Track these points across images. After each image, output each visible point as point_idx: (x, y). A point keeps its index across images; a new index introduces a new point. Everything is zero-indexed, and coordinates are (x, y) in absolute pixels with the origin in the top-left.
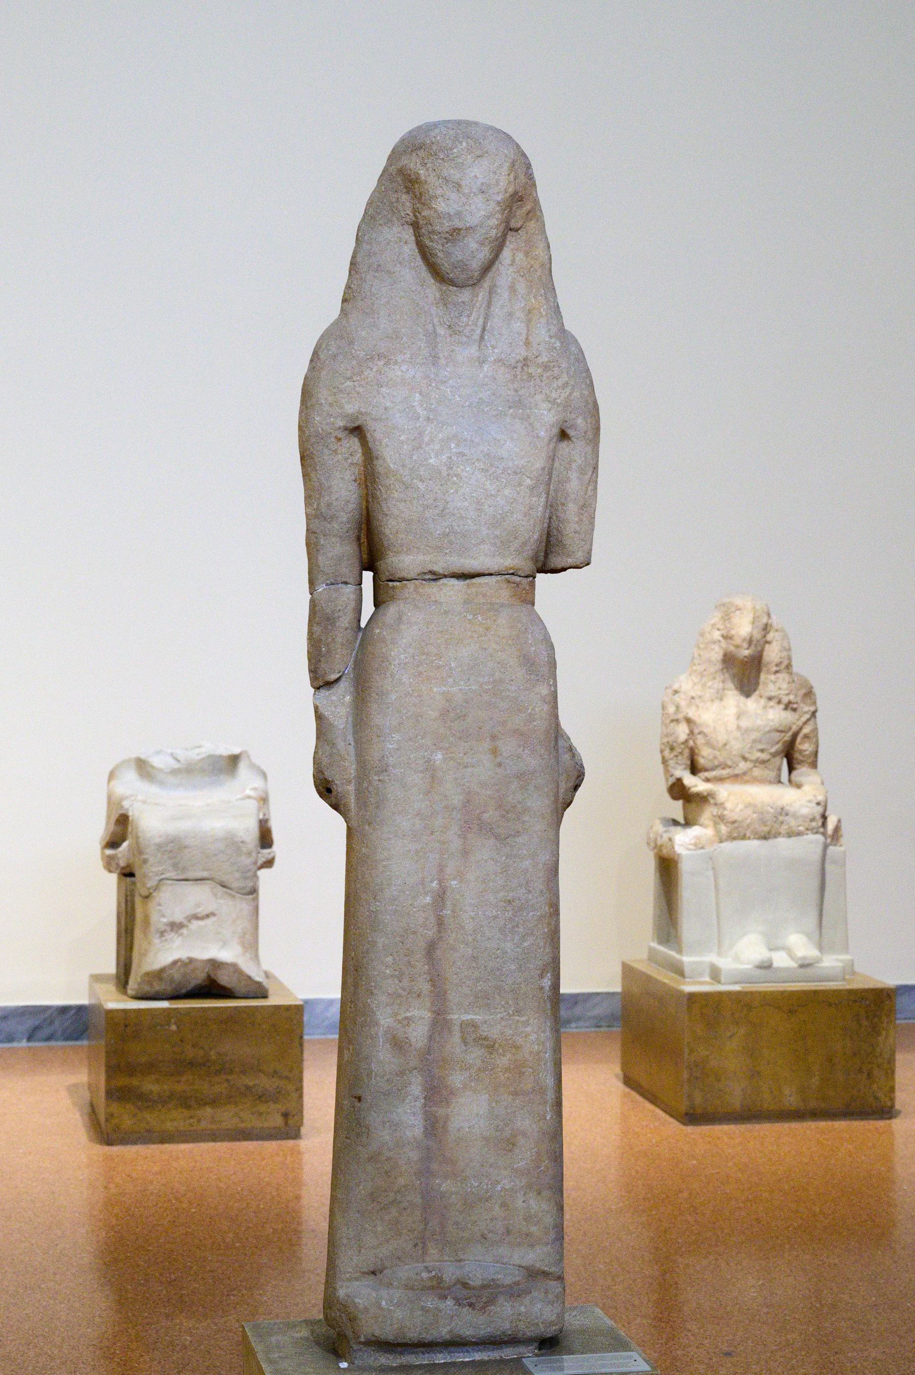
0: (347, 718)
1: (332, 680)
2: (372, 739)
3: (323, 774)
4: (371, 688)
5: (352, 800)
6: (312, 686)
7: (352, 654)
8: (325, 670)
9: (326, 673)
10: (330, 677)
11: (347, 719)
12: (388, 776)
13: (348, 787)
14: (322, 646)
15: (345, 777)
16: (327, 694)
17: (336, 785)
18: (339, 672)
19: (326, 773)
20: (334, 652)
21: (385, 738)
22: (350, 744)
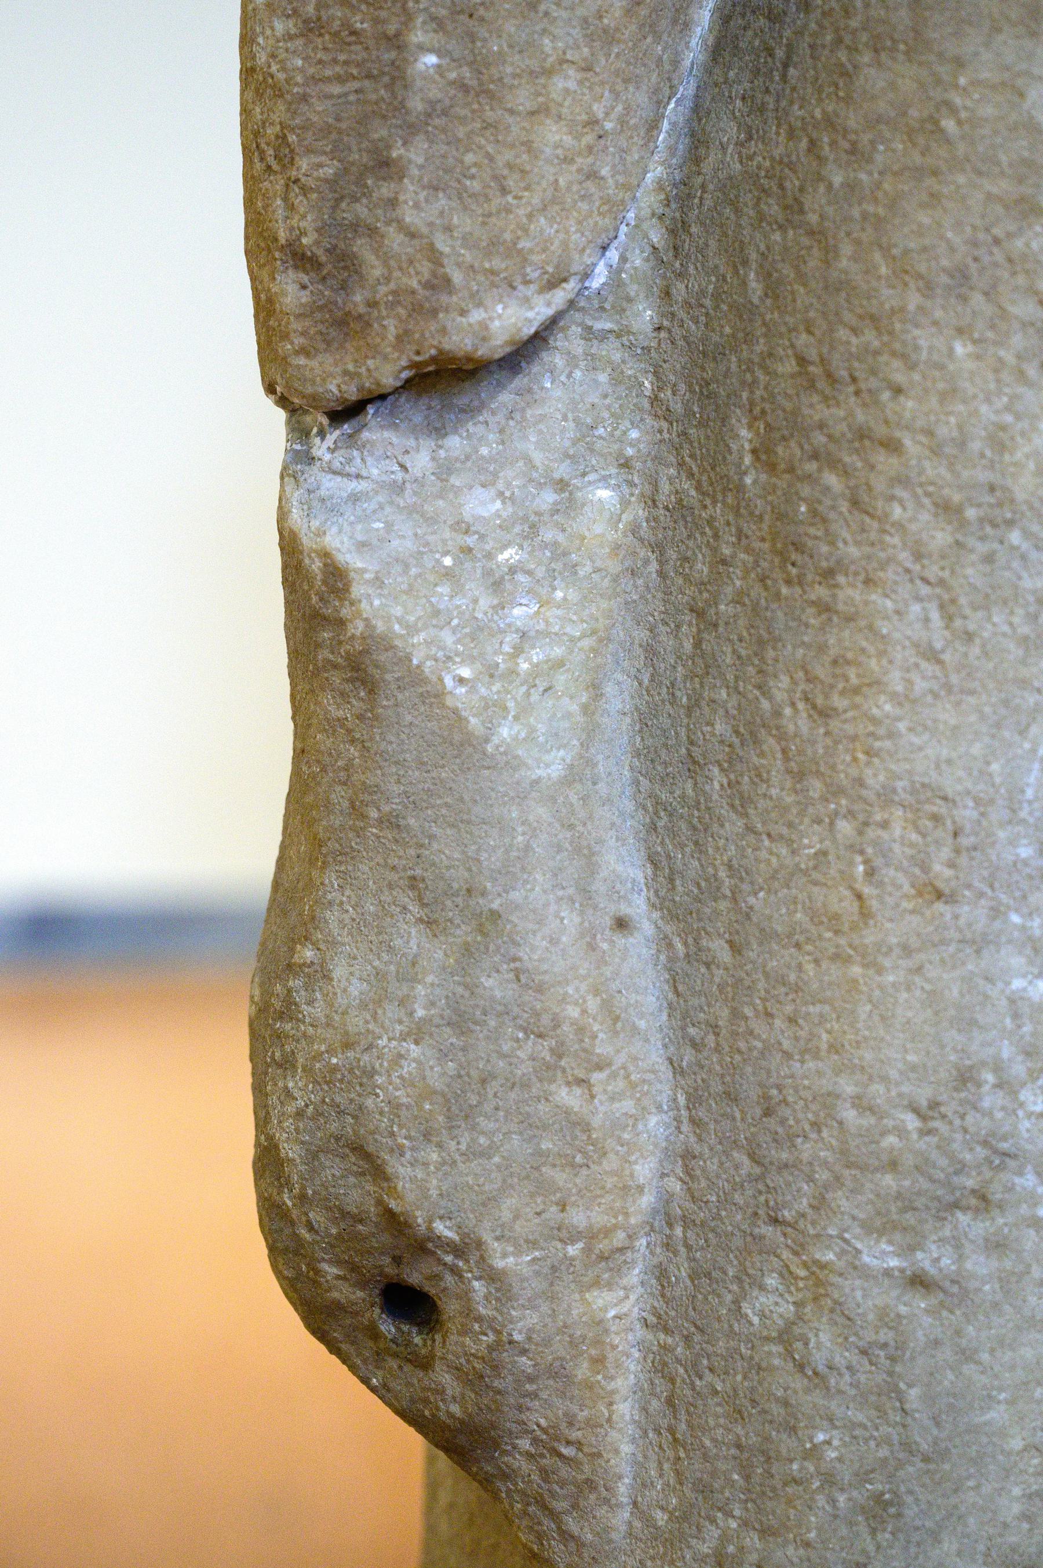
0: (596, 689)
1: (497, 344)
2: (865, 914)
3: (378, 1172)
4: (892, 446)
5: (625, 1409)
6: (270, 389)
7: (653, 126)
8: (435, 257)
9: (440, 283)
10: (476, 316)
11: (596, 689)
12: (997, 1245)
13: (599, 1299)
14: (418, 36)
15: (578, 1218)
16: (421, 461)
17: (493, 1277)
18: (553, 283)
19: (401, 1170)
20: (522, 98)
21: (997, 912)
22: (622, 924)
